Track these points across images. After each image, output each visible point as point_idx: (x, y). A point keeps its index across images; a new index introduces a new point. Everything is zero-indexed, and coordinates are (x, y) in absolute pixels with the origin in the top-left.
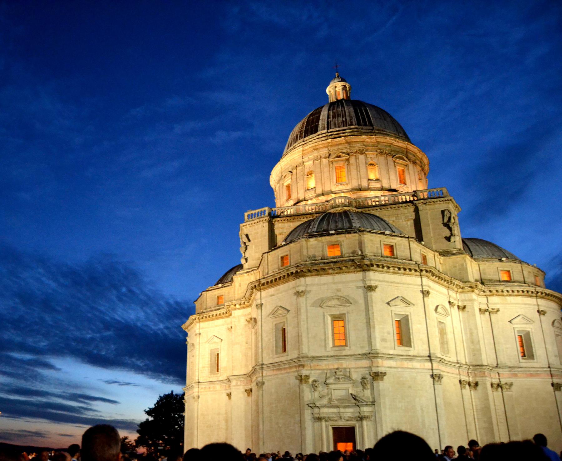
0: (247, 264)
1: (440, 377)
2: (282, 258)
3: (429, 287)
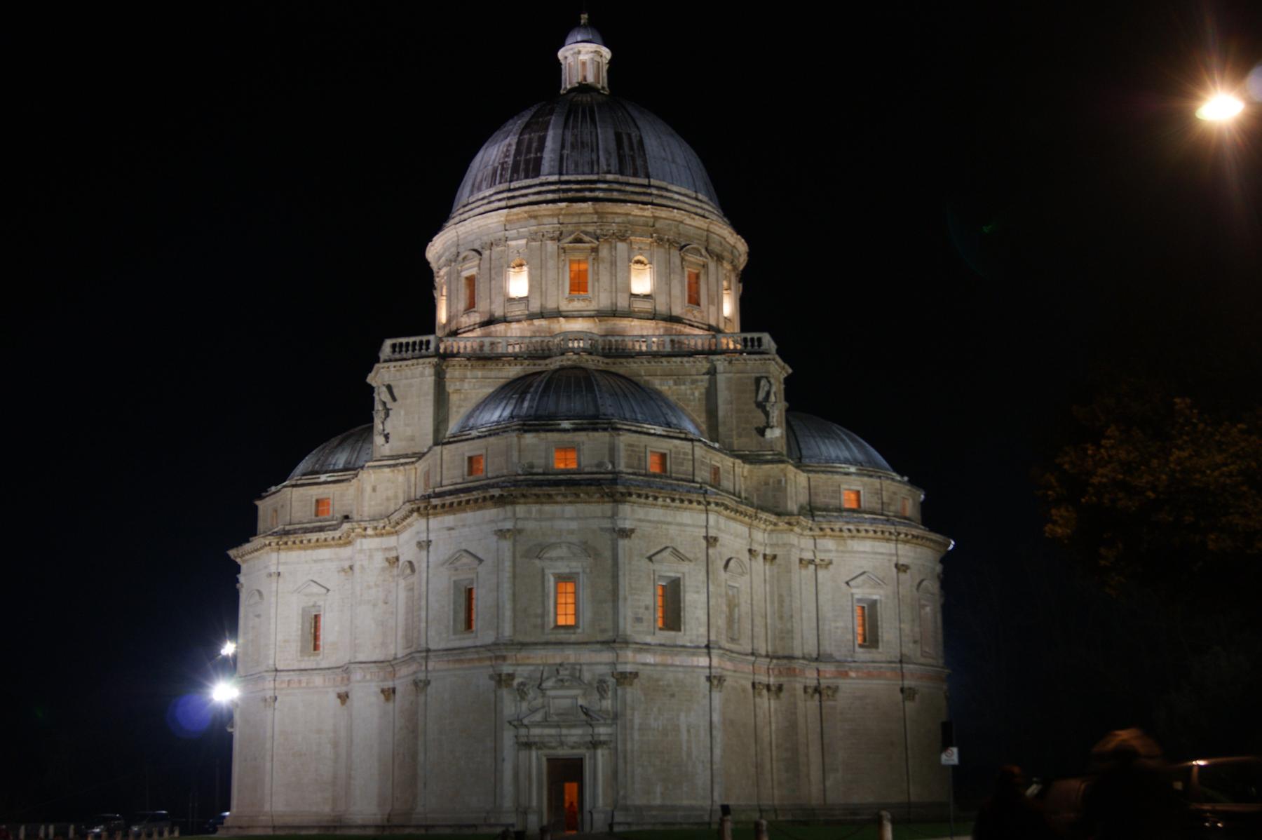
0: (387, 446)
2: (470, 459)
3: (719, 530)
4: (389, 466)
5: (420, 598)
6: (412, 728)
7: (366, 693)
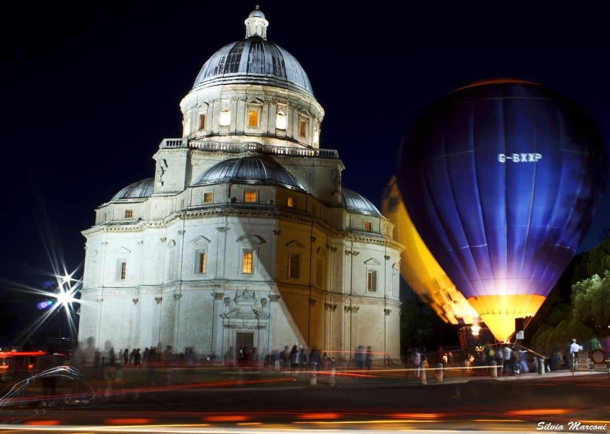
1: (314, 301)
2: (206, 195)
4: (164, 196)
5: (179, 257)
6: (172, 317)
7: (147, 299)
